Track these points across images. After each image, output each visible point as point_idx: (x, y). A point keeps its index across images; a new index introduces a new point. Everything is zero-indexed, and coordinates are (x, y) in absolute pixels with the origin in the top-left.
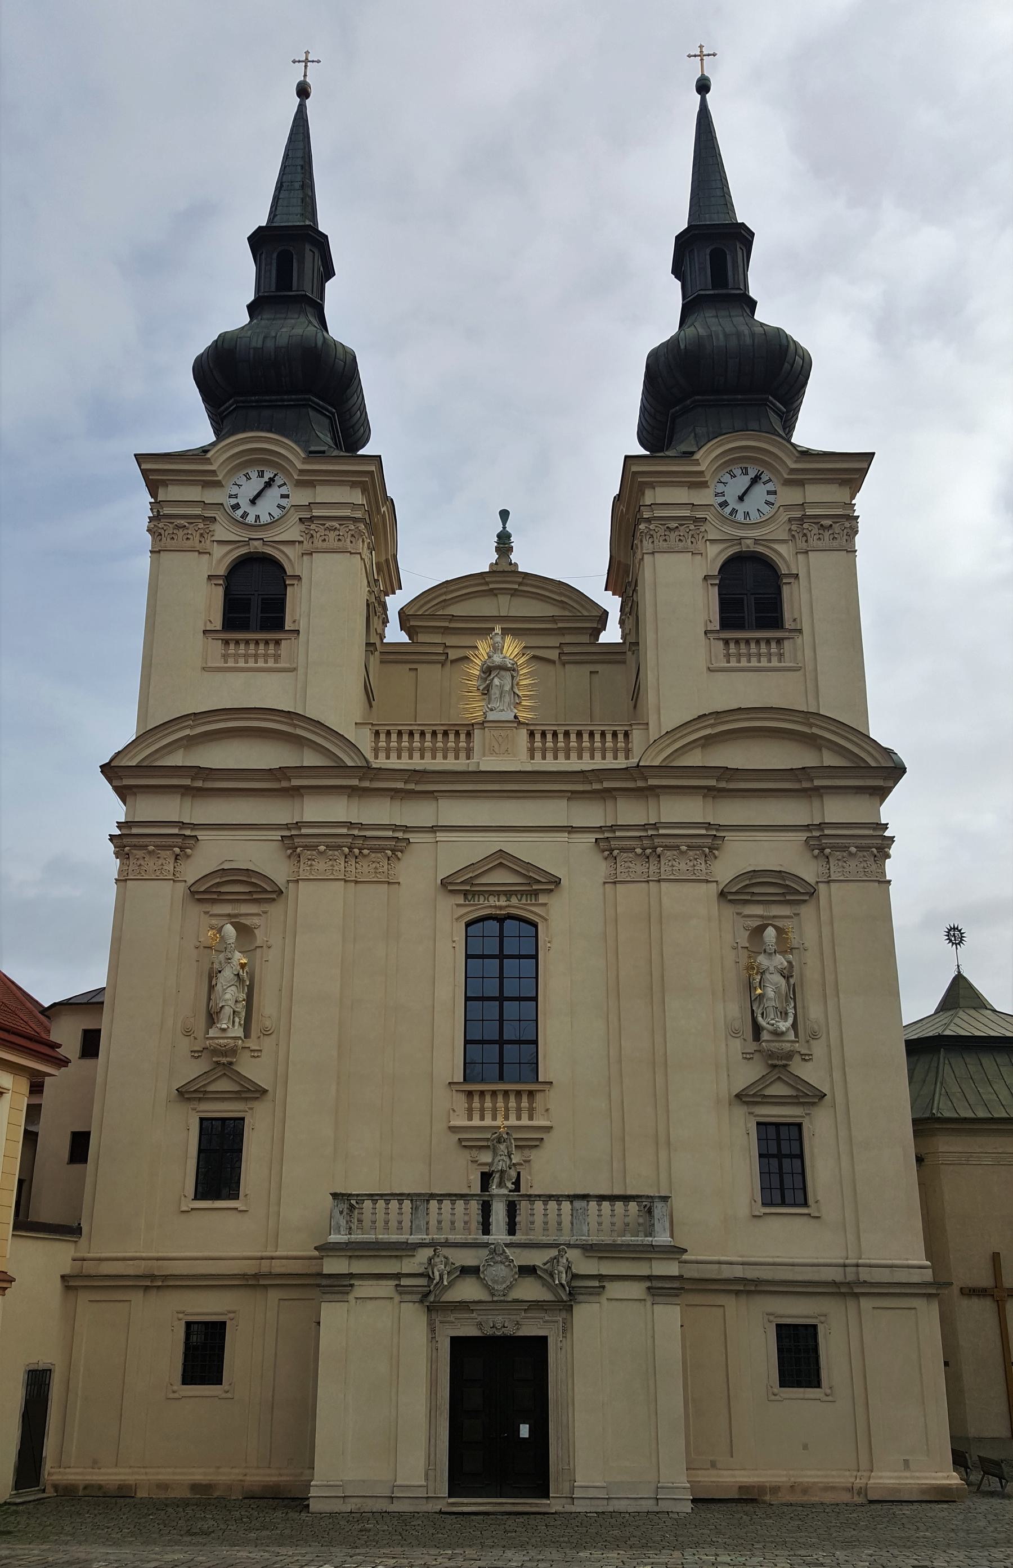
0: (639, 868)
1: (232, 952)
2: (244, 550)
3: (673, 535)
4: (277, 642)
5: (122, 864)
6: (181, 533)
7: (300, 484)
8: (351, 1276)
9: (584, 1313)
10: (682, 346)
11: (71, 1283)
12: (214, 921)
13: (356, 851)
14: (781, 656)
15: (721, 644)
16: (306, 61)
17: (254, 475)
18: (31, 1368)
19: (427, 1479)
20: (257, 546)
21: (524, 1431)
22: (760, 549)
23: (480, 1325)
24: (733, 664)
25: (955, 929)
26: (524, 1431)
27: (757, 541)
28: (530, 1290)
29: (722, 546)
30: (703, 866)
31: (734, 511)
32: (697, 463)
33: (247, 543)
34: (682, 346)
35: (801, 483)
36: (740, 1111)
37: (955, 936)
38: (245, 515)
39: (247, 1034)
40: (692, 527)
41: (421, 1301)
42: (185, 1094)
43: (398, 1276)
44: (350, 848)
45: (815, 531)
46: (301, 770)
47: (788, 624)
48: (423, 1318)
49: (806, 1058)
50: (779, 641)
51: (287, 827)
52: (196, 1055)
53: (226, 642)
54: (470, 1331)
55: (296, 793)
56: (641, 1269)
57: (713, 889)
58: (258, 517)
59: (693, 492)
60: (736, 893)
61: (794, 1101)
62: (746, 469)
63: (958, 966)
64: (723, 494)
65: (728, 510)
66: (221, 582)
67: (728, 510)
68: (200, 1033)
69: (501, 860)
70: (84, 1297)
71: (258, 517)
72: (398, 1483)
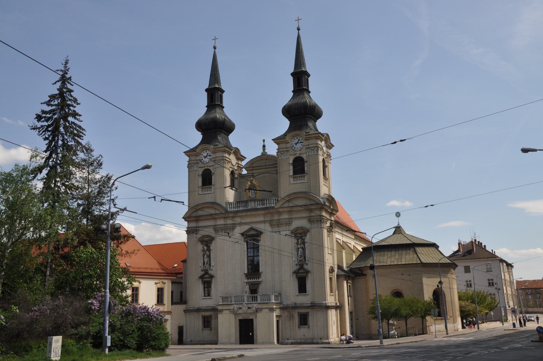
0: (276, 229)
1: (206, 252)
2: (204, 169)
3: (283, 155)
4: (211, 187)
5: (187, 236)
6: (193, 167)
7: (213, 153)
8: (222, 310)
9: (259, 315)
10: (286, 108)
11: (186, 311)
12: (203, 246)
13: (226, 230)
14: (304, 179)
15: (293, 178)
16: (215, 39)
17: (205, 152)
18: (179, 326)
19: (235, 342)
20: (206, 168)
21: (251, 334)
22: (300, 156)
23: (243, 317)
24: (295, 182)
25: (398, 213)
26: (251, 334)
27: (299, 154)
28: (250, 311)
29: (293, 156)
30: (288, 227)
31: (295, 148)
32: (286, 139)
33: (205, 167)
34: (286, 108)
35: (308, 140)
36: (295, 275)
37: (398, 215)
38: (204, 161)
39: (210, 266)
40: (286, 153)
41: (233, 314)
42: (202, 277)
43: (229, 309)
44: (225, 229)
45: (310, 151)
46: (216, 214)
47: (306, 172)
48: (234, 316)
49: (307, 264)
50: (304, 176)
51: (214, 226)
52: (202, 271)
53: (202, 188)
54: (241, 318)
55: (215, 219)
56: (268, 307)
57: (290, 231)
58: (206, 161)
59: (287, 144)
60: (294, 232)
61: (304, 273)
62: (297, 137)
63: (399, 222)
64: (293, 144)
65: (294, 148)
66: (200, 176)
67: (294, 148)
68: (203, 267)
69: (251, 229)
70: (188, 314)
71: (206, 161)
72: (231, 342)
